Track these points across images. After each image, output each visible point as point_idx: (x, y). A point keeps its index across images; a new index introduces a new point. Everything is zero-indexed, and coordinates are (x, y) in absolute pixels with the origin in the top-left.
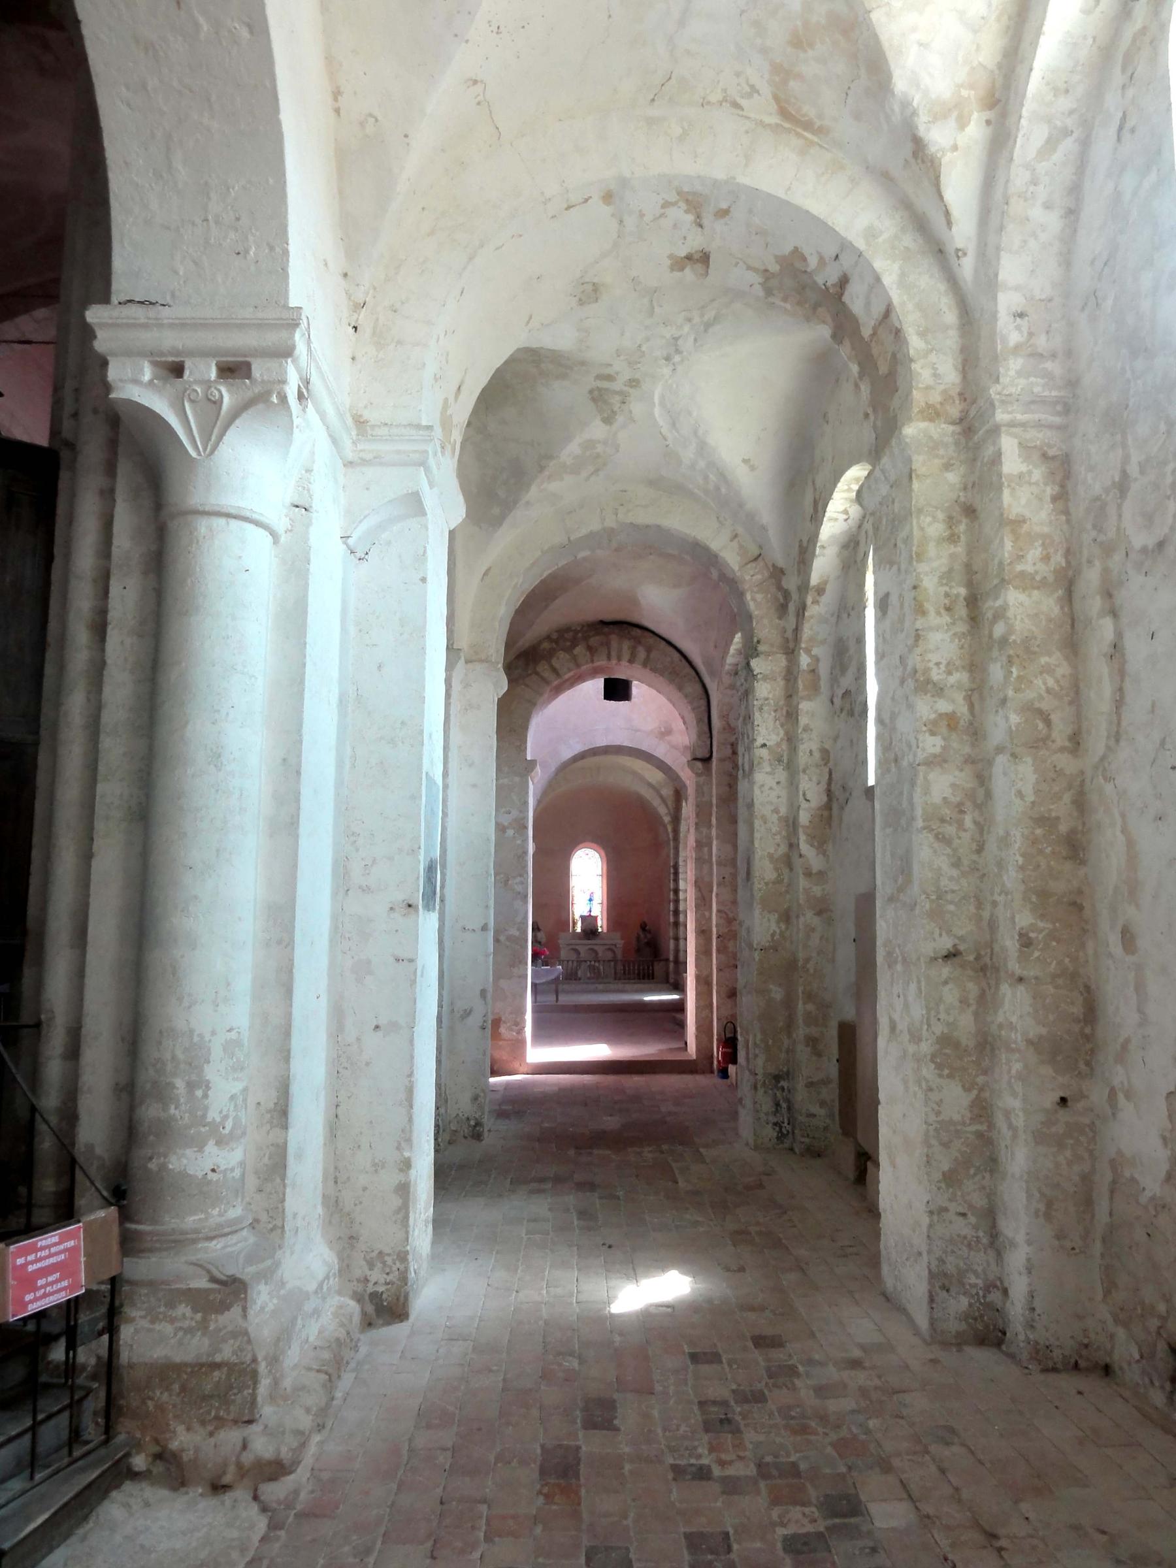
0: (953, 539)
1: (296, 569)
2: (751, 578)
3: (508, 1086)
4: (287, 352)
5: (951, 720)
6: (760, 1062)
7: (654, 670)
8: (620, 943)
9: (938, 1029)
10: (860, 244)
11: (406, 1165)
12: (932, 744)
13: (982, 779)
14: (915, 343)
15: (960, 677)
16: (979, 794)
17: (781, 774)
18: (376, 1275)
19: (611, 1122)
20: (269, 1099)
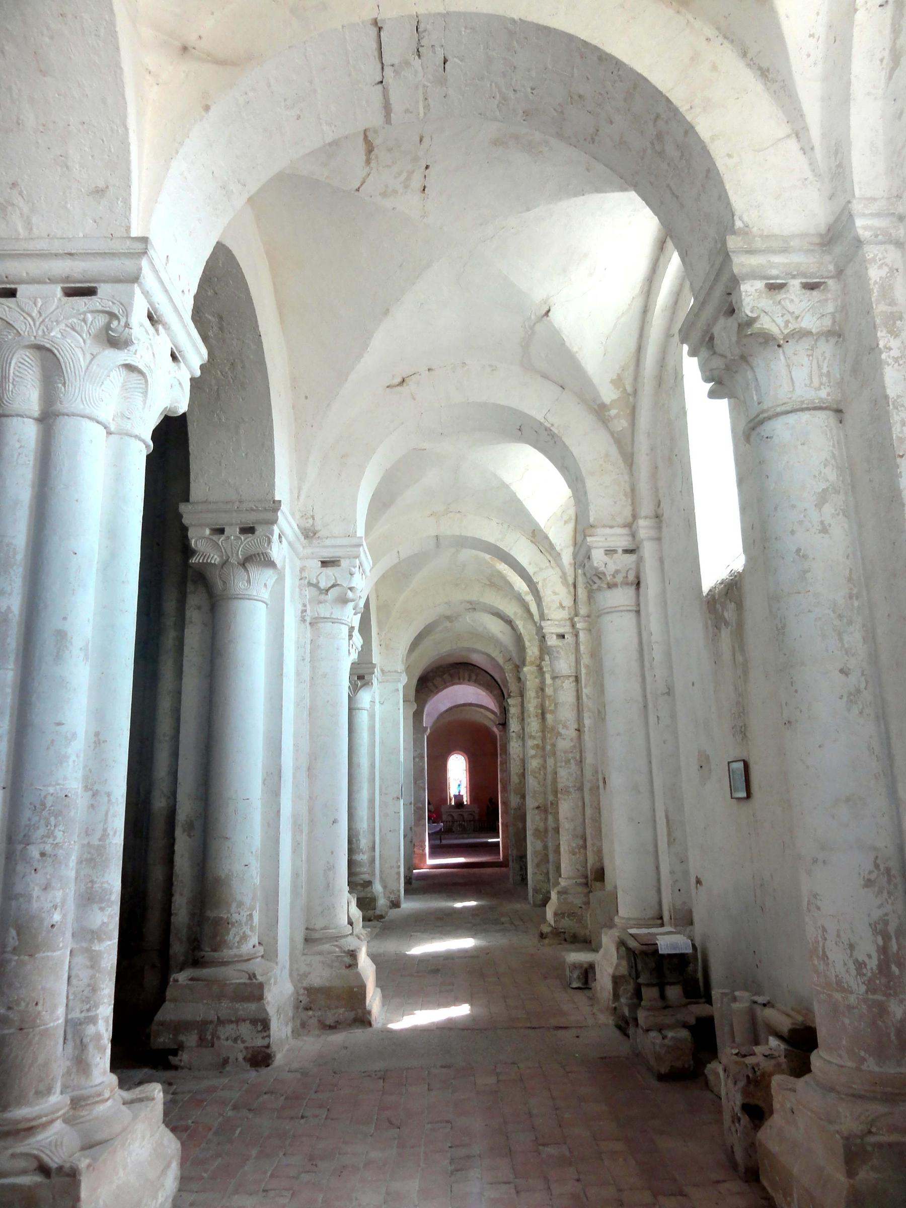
0: (538, 697)
1: (372, 717)
2: (508, 667)
3: (419, 873)
4: (374, 673)
5: (537, 746)
6: (515, 852)
7: (480, 684)
8: (476, 810)
9: (534, 827)
10: (513, 617)
11: (399, 867)
12: (532, 752)
13: (545, 761)
14: (527, 644)
15: (540, 734)
16: (544, 766)
17: (520, 743)
18: (392, 896)
19: (462, 881)
20: (371, 845)
